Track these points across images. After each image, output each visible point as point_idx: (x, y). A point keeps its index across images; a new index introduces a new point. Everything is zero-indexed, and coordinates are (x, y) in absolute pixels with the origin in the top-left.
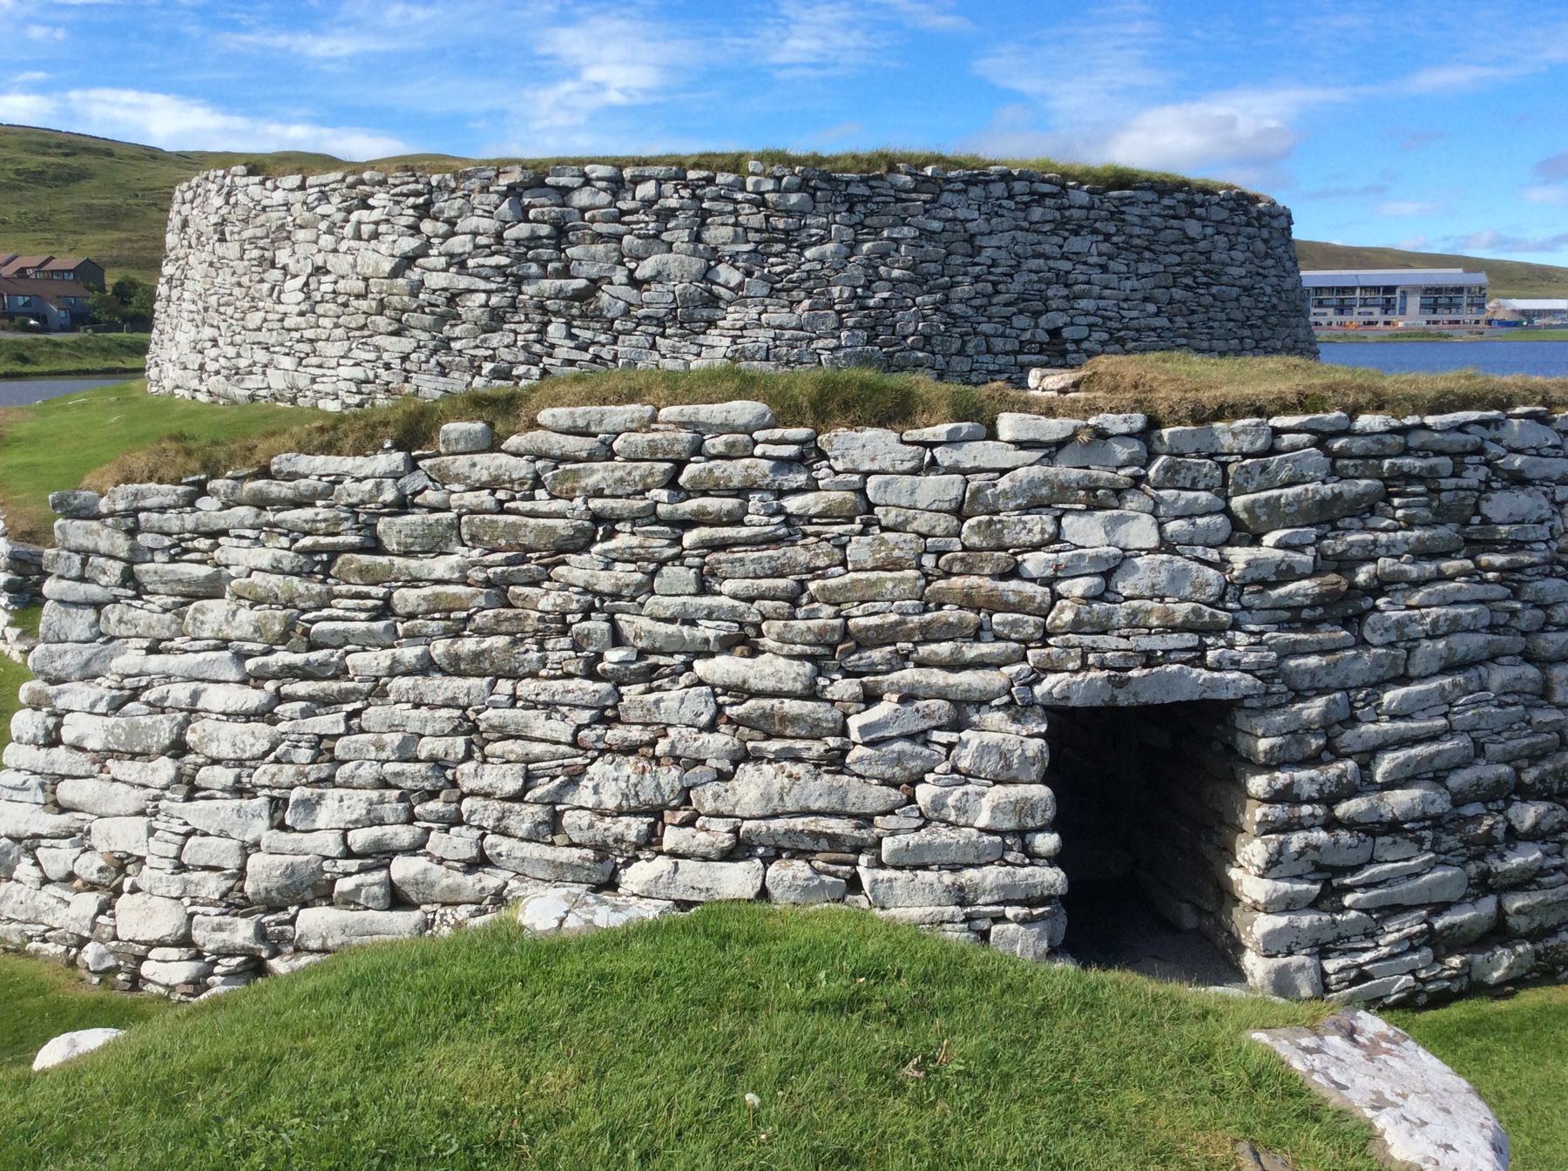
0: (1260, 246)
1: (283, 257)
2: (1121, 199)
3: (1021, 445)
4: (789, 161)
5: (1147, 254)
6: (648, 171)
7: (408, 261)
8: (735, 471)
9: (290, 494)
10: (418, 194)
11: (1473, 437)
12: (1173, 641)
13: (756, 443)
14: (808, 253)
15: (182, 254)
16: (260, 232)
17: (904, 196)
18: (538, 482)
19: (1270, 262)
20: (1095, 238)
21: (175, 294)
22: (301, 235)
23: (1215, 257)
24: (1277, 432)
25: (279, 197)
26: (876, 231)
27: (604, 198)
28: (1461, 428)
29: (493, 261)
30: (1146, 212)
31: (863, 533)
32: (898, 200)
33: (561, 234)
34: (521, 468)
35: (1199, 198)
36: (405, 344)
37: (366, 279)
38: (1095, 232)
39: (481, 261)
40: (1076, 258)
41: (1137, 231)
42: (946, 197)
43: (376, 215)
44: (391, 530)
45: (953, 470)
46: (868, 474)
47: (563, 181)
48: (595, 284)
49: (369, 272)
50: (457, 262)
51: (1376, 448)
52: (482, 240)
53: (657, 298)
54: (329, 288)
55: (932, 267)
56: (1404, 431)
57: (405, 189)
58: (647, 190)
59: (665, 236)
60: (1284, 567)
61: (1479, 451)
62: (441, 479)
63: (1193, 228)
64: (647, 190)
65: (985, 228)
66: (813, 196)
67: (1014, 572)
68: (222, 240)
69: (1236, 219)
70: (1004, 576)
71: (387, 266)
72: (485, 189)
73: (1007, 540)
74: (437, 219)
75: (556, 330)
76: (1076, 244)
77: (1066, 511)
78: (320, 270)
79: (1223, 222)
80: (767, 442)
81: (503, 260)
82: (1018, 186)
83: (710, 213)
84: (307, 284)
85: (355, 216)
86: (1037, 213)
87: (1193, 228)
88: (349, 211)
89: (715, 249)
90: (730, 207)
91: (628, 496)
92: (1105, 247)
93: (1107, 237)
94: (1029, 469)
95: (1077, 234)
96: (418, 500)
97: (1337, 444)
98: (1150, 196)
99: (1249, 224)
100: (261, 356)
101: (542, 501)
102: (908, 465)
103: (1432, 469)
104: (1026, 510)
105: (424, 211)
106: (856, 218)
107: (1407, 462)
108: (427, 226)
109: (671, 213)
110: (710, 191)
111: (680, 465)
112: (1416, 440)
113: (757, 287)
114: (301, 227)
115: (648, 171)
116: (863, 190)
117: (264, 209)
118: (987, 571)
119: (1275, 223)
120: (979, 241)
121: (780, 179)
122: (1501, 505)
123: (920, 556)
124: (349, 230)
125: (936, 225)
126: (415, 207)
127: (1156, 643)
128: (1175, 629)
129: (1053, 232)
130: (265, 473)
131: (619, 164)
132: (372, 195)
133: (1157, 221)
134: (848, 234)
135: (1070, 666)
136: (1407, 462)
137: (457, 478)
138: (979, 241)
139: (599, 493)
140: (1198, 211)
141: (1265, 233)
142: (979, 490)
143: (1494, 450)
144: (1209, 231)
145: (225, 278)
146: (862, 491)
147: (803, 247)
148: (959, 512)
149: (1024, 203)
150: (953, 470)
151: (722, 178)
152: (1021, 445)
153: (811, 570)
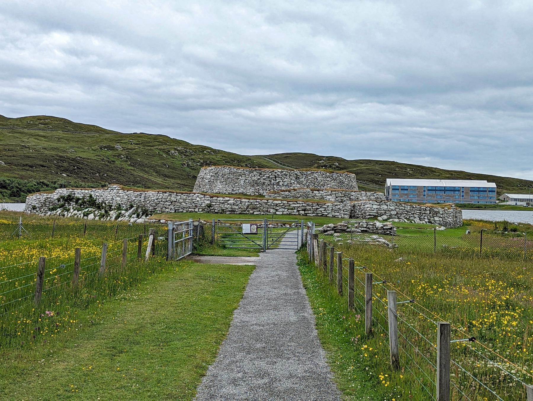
7: (259, 179)
36: (258, 187)
44: (288, 197)
50: (265, 179)
53: (286, 183)
63: (341, 177)
76: (328, 179)
87: (341, 177)
94: (325, 194)
105: (261, 174)
109: (286, 175)
113: (296, 183)
122: (351, 197)
145: (230, 180)
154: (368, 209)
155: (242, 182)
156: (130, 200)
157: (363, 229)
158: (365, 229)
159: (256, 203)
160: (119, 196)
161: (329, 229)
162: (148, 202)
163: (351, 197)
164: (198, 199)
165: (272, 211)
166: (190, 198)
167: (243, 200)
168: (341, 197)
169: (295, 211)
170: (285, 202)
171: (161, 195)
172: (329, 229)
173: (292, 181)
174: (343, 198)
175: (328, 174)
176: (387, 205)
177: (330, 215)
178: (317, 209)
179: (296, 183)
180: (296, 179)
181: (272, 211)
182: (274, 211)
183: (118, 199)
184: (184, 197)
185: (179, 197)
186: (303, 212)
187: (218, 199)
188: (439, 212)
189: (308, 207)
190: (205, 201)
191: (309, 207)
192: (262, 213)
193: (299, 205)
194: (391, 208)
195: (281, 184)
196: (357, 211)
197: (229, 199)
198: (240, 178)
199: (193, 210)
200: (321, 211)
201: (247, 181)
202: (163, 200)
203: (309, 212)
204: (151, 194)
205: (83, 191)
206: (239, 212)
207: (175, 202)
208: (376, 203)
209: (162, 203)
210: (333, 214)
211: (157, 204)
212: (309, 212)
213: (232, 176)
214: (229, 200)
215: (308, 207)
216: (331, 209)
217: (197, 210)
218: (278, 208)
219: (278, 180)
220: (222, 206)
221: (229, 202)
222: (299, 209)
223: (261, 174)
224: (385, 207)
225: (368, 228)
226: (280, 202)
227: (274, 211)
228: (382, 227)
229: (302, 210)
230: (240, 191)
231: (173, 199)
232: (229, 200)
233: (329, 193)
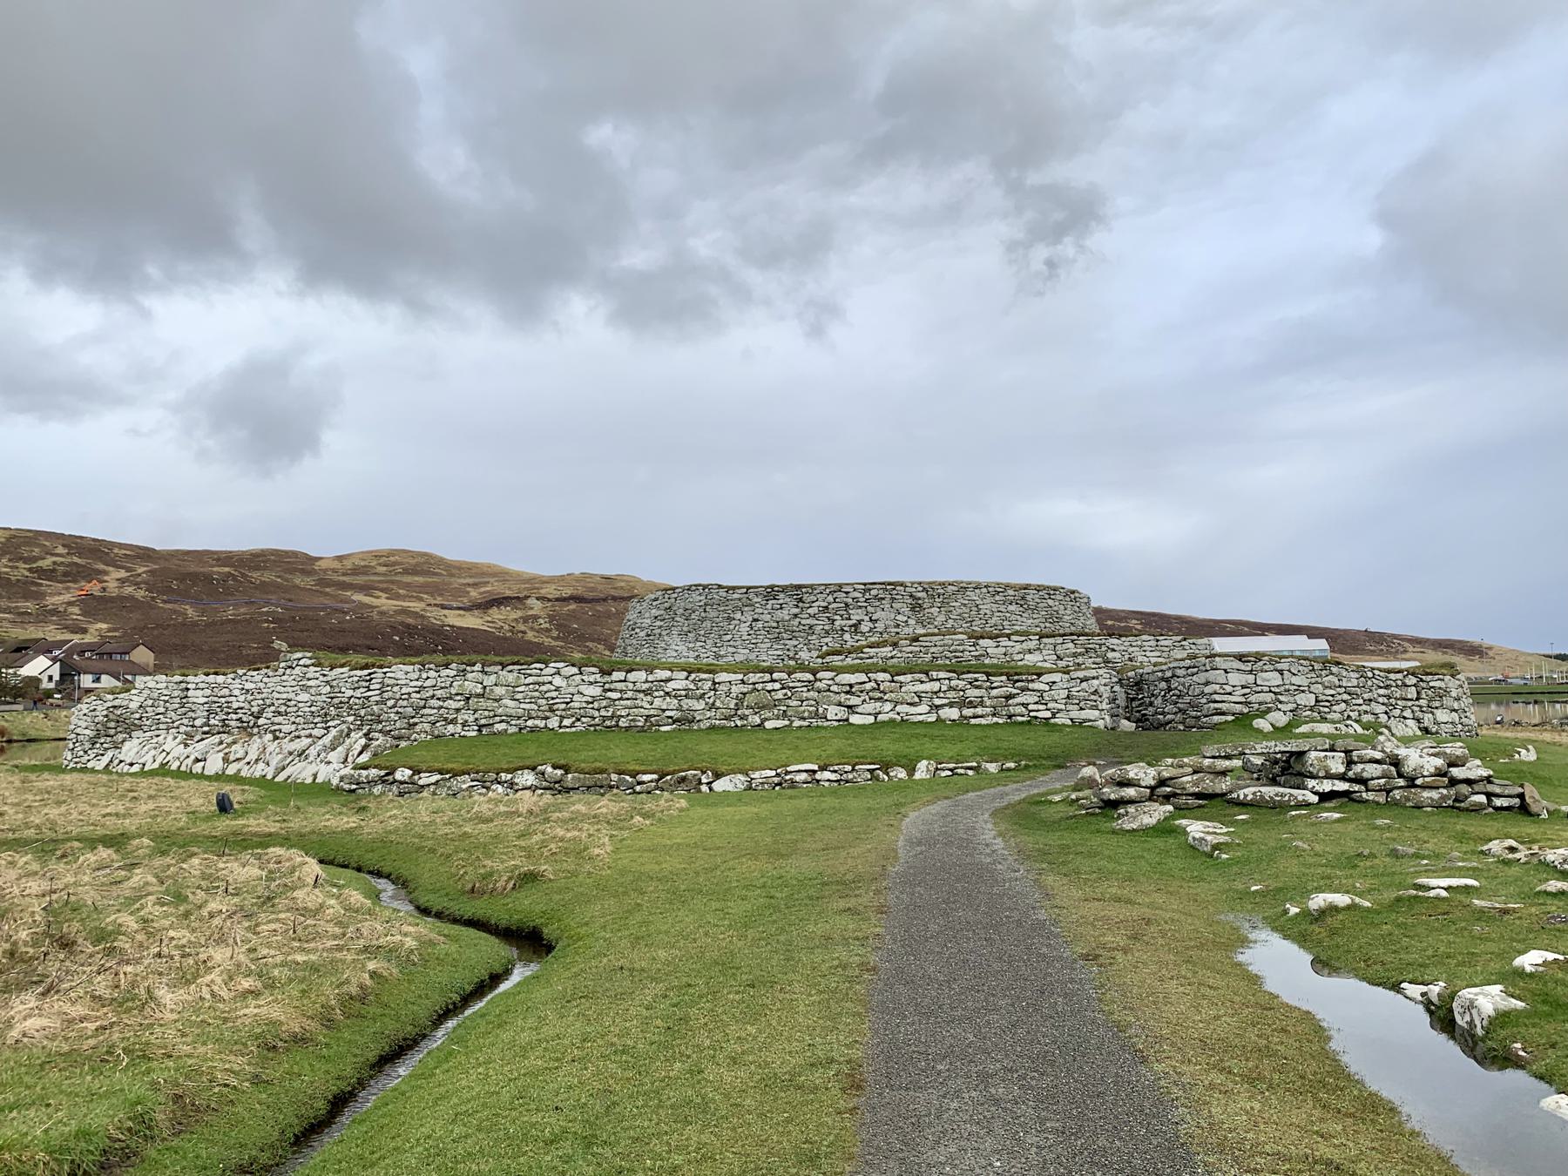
7: (796, 616)
40: (1011, 612)
48: (860, 622)
53: (880, 626)
58: (874, 592)
64: (874, 592)
75: (847, 636)
76: (1011, 608)
78: (756, 620)
94: (1018, 647)
100: (731, 650)
105: (801, 600)
113: (912, 622)
122: (1110, 655)
145: (708, 624)
154: (1208, 690)
155: (744, 628)
156: (336, 701)
157: (1327, 786)
158: (1342, 786)
159: (769, 686)
160: (305, 688)
161: (1131, 792)
162: (390, 703)
163: (1110, 655)
164: (558, 681)
165: (834, 712)
166: (530, 680)
167: (722, 677)
168: (1075, 655)
169: (924, 708)
170: (881, 676)
171: (432, 674)
172: (1131, 792)
173: (900, 617)
175: (1011, 592)
176: (1281, 672)
177: (1061, 720)
178: (1009, 697)
179: (912, 622)
180: (913, 609)
181: (834, 712)
182: (842, 713)
183: (304, 697)
184: (511, 678)
185: (493, 678)
186: (953, 713)
187: (632, 676)
188: (1447, 691)
189: (972, 693)
190: (582, 688)
191: (977, 692)
192: (797, 723)
193: (935, 686)
194: (1295, 680)
195: (864, 628)
196: (1158, 702)
197: (667, 674)
198: (738, 616)
199: (541, 724)
200: (1025, 705)
201: (760, 625)
202: (439, 693)
203: (979, 711)
204: (400, 675)
205: (211, 678)
206: (705, 725)
207: (478, 696)
208: (1237, 664)
209: (434, 703)
210: (1075, 714)
211: (418, 709)
212: (979, 711)
213: (713, 614)
214: (668, 680)
215: (972, 693)
216: (1064, 693)
217: (553, 723)
218: (854, 701)
219: (855, 618)
220: (644, 701)
221: (671, 686)
222: (937, 702)
223: (801, 600)
224: (1273, 679)
225: (1362, 781)
226: (862, 677)
227: (842, 713)
228: (1440, 773)
229: (951, 705)
230: (739, 658)
231: (471, 687)
232: (668, 680)
233: (1032, 644)
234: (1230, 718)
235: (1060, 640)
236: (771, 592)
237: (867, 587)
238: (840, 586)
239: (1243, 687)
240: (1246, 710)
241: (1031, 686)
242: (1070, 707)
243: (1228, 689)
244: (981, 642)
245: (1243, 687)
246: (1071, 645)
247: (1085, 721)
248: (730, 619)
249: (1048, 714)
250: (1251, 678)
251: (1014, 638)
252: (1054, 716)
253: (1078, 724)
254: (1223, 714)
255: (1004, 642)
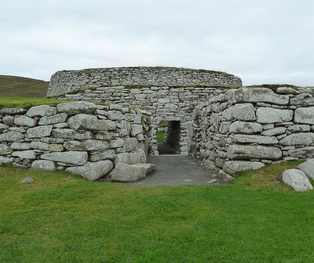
0: (231, 83)
1: (68, 84)
2: (203, 74)
3: (154, 90)
4: (147, 68)
5: (207, 83)
6: (124, 69)
8: (119, 94)
9: (67, 99)
10: (89, 73)
11: (212, 91)
12: (171, 113)
13: (122, 91)
14: (149, 81)
15: (52, 86)
16: (64, 80)
17: (165, 72)
18: (96, 96)
19: (232, 85)
20: (198, 80)
21: (50, 92)
22: (71, 80)
23: (221, 84)
24: (185, 90)
25: (68, 75)
26: (160, 77)
27: (117, 73)
28: (210, 90)
29: (100, 83)
30: (207, 76)
31: (134, 101)
32: (164, 73)
33: (110, 78)
34: (94, 95)
35: (217, 74)
37: (80, 86)
38: (198, 79)
39: (98, 83)
41: (206, 79)
42: (172, 73)
43: (82, 77)
45: (145, 93)
46: (135, 94)
47: (111, 71)
49: (81, 85)
50: (94, 83)
51: (198, 92)
52: (98, 80)
54: (75, 88)
55: (169, 83)
56: (202, 90)
57: (87, 72)
58: (123, 72)
59: (126, 78)
60: (185, 105)
61: (213, 93)
62: (85, 96)
63: (216, 79)
64: (123, 72)
65: (178, 78)
66: (150, 72)
67: (152, 105)
68: (59, 82)
69: (225, 78)
70: (151, 106)
71: (84, 84)
72: (99, 72)
73: (151, 101)
74: (92, 77)
76: (194, 81)
77: (159, 98)
78: (74, 86)
79: (222, 78)
80: (123, 91)
81: (101, 82)
82: (184, 71)
83: (133, 75)
84: (71, 88)
85: (79, 77)
86: (187, 75)
88: (79, 77)
89: (134, 80)
90: (137, 74)
91: (107, 97)
92: (200, 81)
93: (200, 80)
94: (154, 94)
95: (195, 79)
96: (82, 99)
97: (192, 91)
98: (208, 74)
99: (228, 79)
101: (96, 99)
102: (139, 93)
103: (205, 95)
104: (154, 98)
105: (90, 76)
106: (157, 76)
107: (202, 94)
108: (90, 78)
109: (128, 75)
110: (134, 71)
111: (113, 93)
112: (203, 91)
114: (71, 79)
115: (124, 69)
116: (158, 71)
117: (66, 77)
118: (149, 105)
119: (234, 79)
120: (177, 79)
121: (144, 70)
123: (141, 103)
124: (78, 79)
125: (170, 77)
126: (88, 75)
127: (169, 113)
128: (171, 112)
129: (190, 79)
130: (65, 97)
131: (120, 68)
132: (82, 74)
133: (210, 78)
134: (155, 78)
135: (158, 116)
136: (202, 94)
137: (87, 96)
138: (177, 79)
139: (103, 97)
140: (217, 76)
141: (231, 81)
142: (148, 96)
143: (214, 92)
144: (219, 80)
146: (134, 96)
147: (148, 80)
148: (146, 98)
149: (186, 74)
150: (145, 93)
151: (135, 70)
152: (154, 90)
153: (128, 105)
168: (191, 99)
174: (195, 102)
175: (195, 73)
216: (47, 130)
223: (90, 76)
233: (163, 92)
234: (257, 165)
235: (182, 90)
236: (79, 73)
237: (120, 70)
238: (108, 69)
239: (276, 125)
240: (277, 154)
241: (19, 120)
242: (53, 147)
243: (256, 127)
244: (133, 91)
245: (276, 125)
246: (189, 93)
247: (68, 165)
248: (65, 85)
249: (30, 154)
250: (287, 114)
251: (152, 88)
252: (38, 156)
253: (62, 169)
254: (247, 159)
255: (147, 91)
